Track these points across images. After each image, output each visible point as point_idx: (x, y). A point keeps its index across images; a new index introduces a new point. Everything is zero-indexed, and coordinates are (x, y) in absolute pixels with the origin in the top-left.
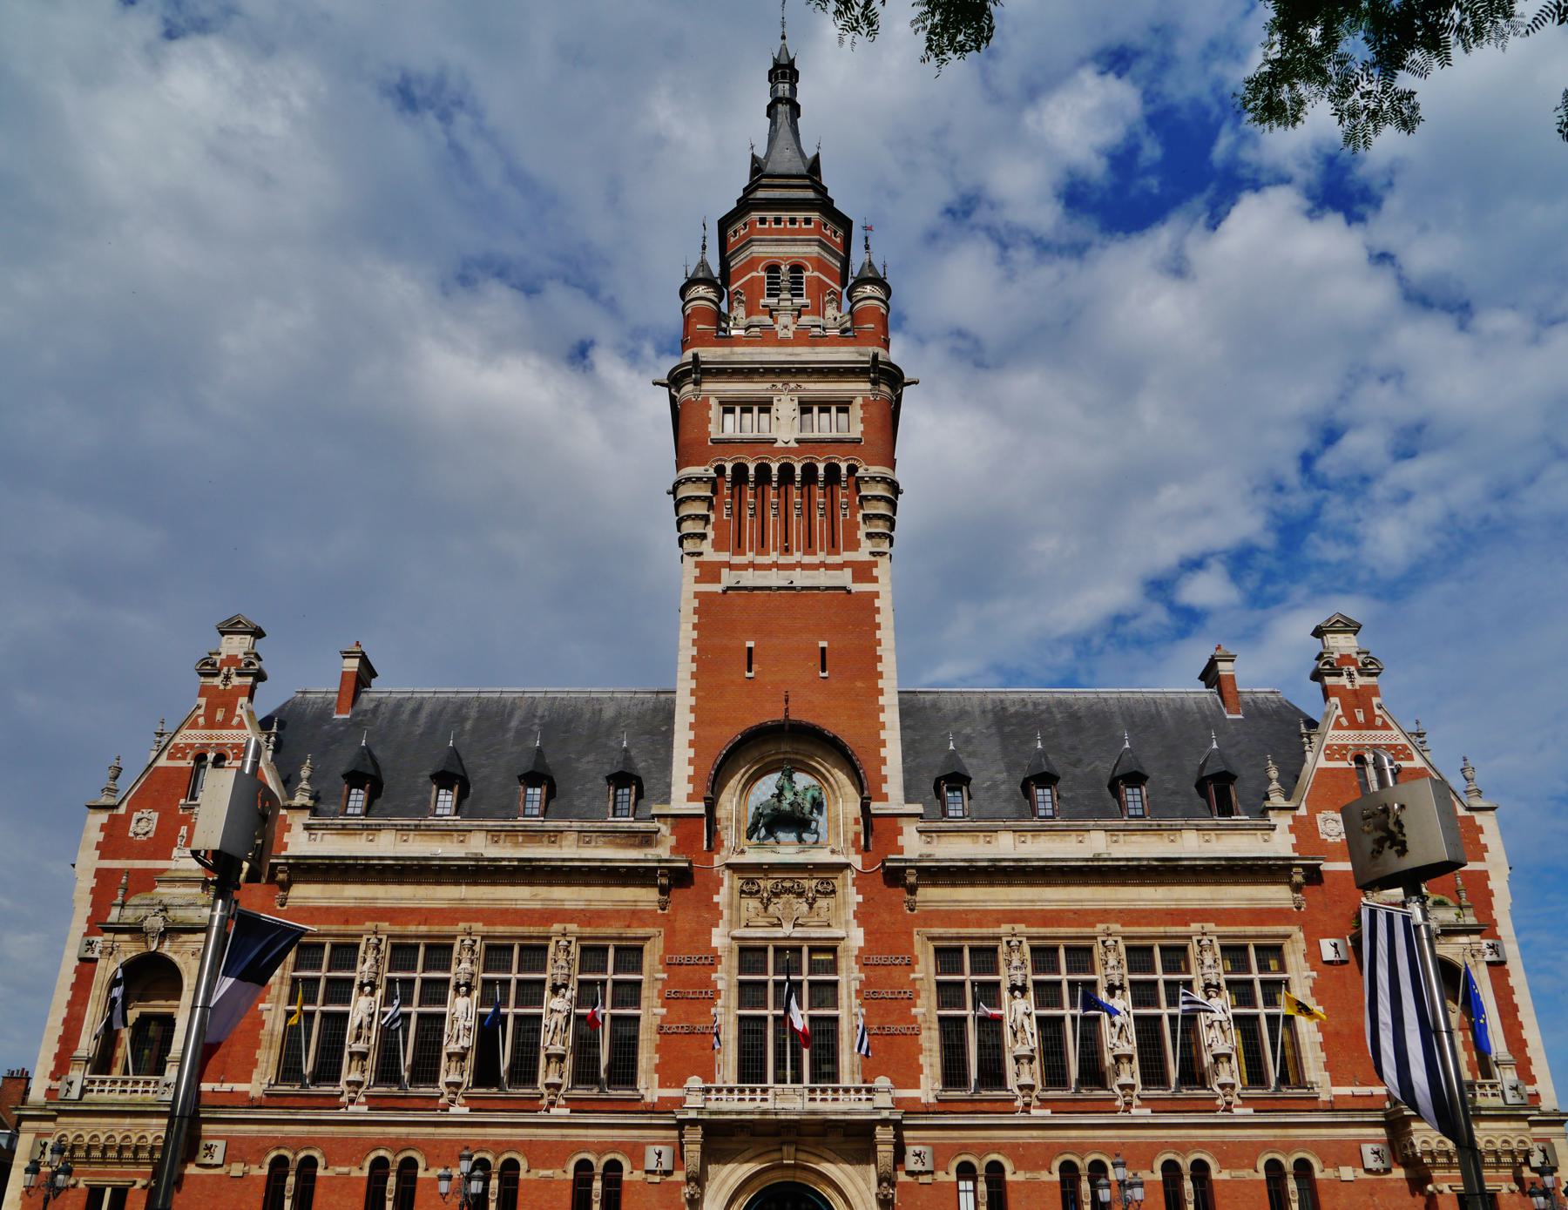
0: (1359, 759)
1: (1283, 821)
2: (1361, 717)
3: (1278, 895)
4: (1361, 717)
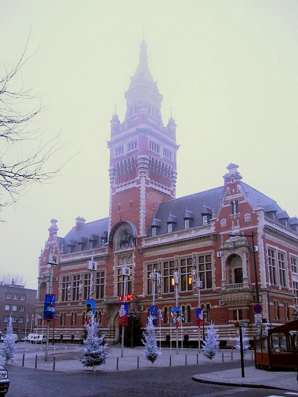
0: (232, 203)
1: (213, 224)
2: (233, 191)
3: (209, 243)
4: (233, 191)
